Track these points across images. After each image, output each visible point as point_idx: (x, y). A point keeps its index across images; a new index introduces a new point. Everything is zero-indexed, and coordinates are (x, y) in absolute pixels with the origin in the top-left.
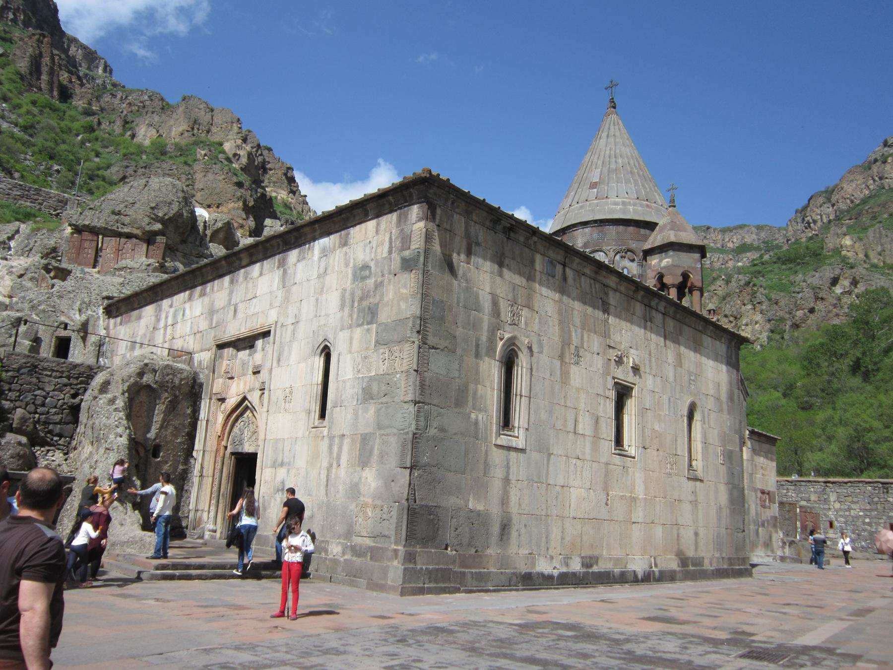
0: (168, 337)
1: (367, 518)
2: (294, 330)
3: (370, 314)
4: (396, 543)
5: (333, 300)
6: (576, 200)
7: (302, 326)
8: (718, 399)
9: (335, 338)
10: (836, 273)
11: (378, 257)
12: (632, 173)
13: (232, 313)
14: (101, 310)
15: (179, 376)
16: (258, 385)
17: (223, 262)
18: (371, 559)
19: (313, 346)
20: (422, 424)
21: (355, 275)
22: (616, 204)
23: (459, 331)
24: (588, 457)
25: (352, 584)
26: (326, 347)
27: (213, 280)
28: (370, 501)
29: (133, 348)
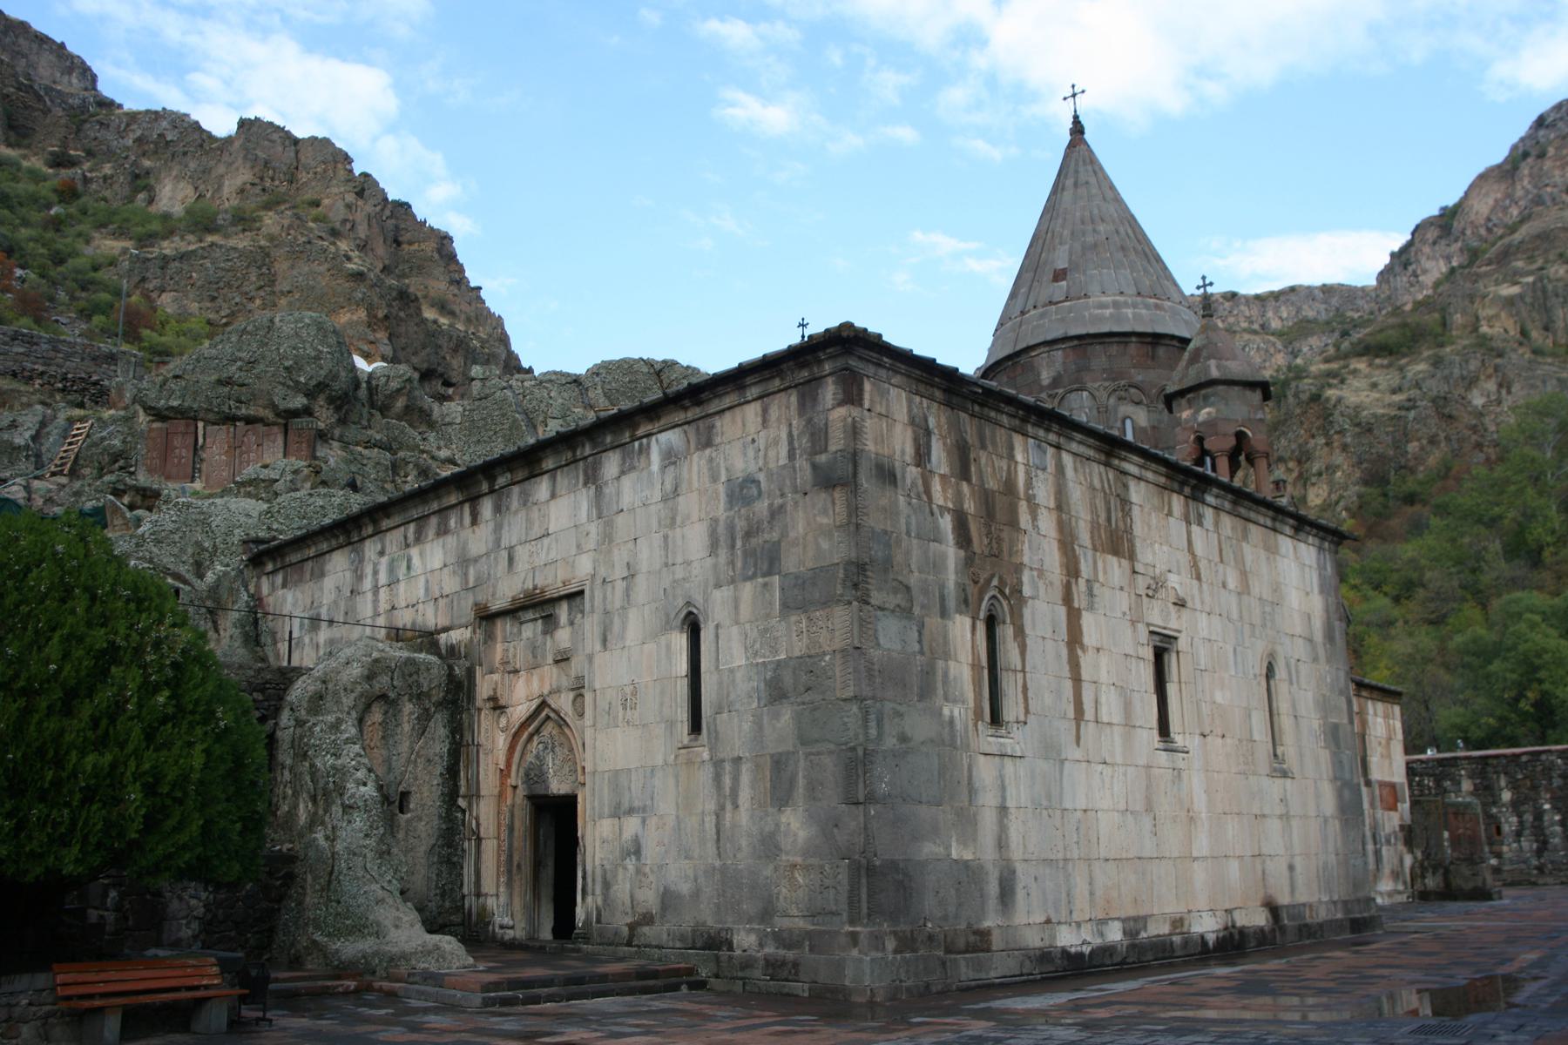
0: (383, 606)
4: (852, 922)
5: (694, 539)
6: (1031, 303)
7: (641, 583)
8: (1310, 641)
9: (706, 601)
10: (1472, 368)
11: (772, 465)
12: (1123, 248)
13: (504, 562)
18: (811, 950)
19: (667, 615)
20: (873, 732)
22: (1103, 306)
23: (914, 580)
24: (1119, 759)
28: (799, 860)
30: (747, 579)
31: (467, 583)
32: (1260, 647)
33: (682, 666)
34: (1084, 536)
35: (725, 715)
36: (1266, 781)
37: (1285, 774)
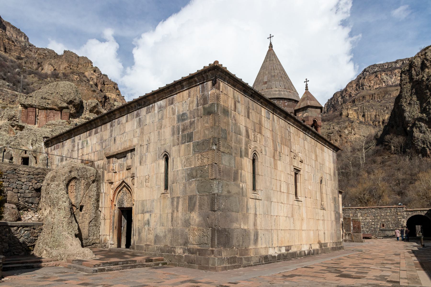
1: (194, 235)
2: (147, 148)
3: (190, 137)
5: (167, 132)
9: (170, 150)
11: (191, 109)
14: (43, 144)
15: (89, 172)
16: (130, 175)
17: (106, 117)
18: (199, 255)
21: (179, 120)
23: (233, 145)
24: (285, 202)
25: (189, 267)
26: (165, 155)
27: (101, 125)
29: (62, 160)
30: (182, 143)
31: (103, 147)
32: (319, 175)
33: (163, 170)
34: (279, 140)
35: (175, 184)
36: (319, 211)
37: (324, 209)
